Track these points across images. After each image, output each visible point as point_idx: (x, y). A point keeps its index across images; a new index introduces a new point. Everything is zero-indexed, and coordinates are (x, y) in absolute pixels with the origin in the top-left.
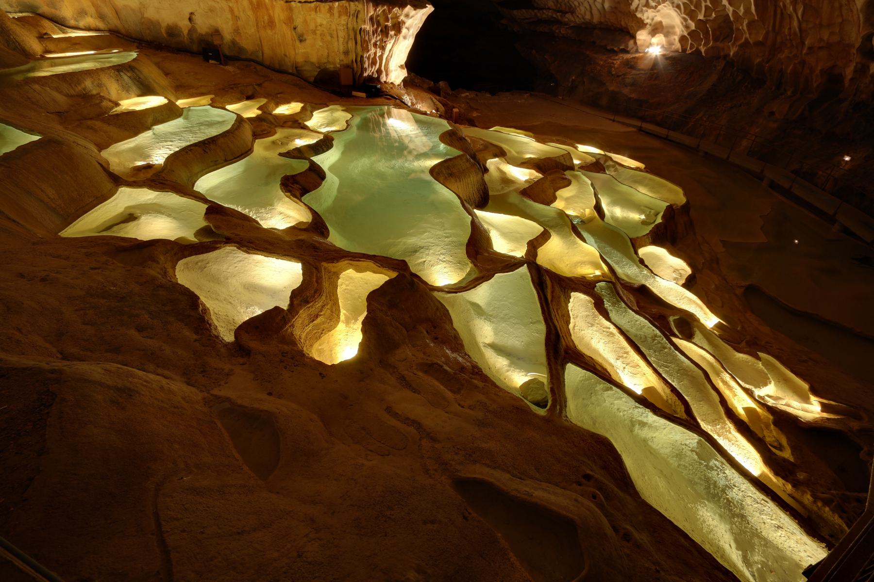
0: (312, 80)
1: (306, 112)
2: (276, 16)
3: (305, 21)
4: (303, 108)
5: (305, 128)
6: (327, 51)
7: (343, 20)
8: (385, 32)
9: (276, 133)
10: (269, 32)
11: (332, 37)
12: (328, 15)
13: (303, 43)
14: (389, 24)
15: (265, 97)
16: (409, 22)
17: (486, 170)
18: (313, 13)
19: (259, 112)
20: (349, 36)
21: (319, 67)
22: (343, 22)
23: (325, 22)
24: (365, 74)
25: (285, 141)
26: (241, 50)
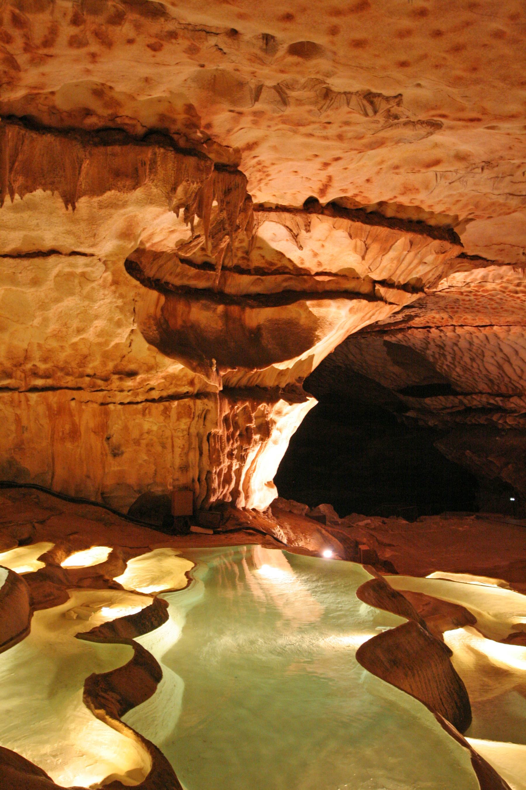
0: (125, 511)
1: (117, 562)
2: (83, 423)
3: (126, 428)
4: (111, 556)
5: (118, 587)
6: (153, 467)
7: (184, 423)
8: (246, 437)
9: (67, 598)
10: (69, 445)
11: (164, 447)
12: (162, 418)
13: (118, 459)
14: (253, 425)
15: (49, 541)
16: (280, 422)
17: (448, 652)
18: (140, 416)
19: (42, 565)
20: (190, 444)
21: (139, 491)
23: (155, 428)
24: (213, 499)
25: (83, 611)
26: (21, 472)
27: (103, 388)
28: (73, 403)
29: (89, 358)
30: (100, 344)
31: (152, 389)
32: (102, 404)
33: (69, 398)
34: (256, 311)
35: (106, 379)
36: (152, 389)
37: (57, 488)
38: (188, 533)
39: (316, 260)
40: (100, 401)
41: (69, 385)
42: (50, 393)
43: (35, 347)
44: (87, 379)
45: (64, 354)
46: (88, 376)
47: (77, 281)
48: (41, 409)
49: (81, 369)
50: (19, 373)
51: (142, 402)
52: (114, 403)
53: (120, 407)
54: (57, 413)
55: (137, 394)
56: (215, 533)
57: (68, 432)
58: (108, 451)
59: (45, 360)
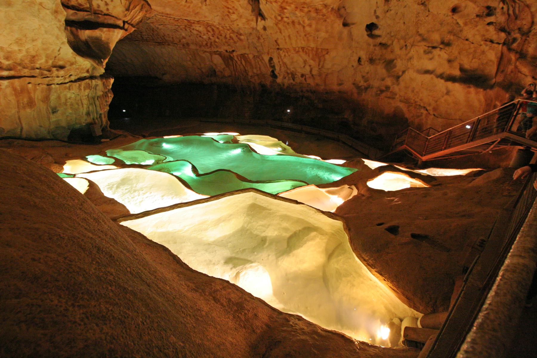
2: (36, 96)
3: (59, 97)
7: (87, 92)
10: (28, 110)
11: (78, 104)
13: (55, 114)
18: (67, 90)
21: (69, 129)
22: (87, 94)
23: (73, 96)
28: (30, 86)
29: (37, 58)
30: (45, 49)
31: (71, 75)
32: (48, 85)
34: (83, 31)
36: (71, 75)
37: (24, 135)
38: (101, 143)
39: (106, 7)
40: (47, 83)
41: (26, 75)
42: (16, 80)
44: (38, 70)
45: (21, 55)
46: (37, 69)
47: (37, 7)
48: (9, 91)
49: (32, 65)
51: (67, 83)
53: (58, 86)
55: (65, 79)
56: (111, 140)
57: (26, 102)
58: (51, 111)
59: (7, 58)
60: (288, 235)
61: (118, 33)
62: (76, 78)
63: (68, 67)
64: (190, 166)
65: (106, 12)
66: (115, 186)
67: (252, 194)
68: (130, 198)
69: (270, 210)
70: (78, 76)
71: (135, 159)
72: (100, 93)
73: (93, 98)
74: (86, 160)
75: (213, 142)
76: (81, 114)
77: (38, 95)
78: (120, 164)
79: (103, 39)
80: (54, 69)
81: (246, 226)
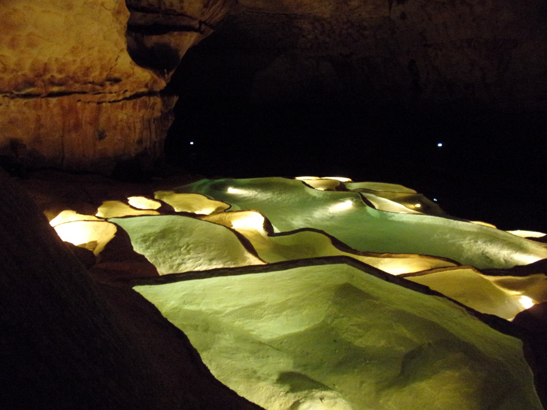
3: (109, 118)
10: (73, 135)
12: (132, 110)
18: (120, 110)
22: (141, 115)
27: (101, 91)
28: (79, 104)
29: (91, 69)
31: (126, 91)
33: (77, 100)
35: (102, 85)
36: (126, 91)
40: (97, 101)
43: (53, 62)
44: (90, 85)
46: (90, 83)
48: (56, 110)
49: (85, 78)
50: (40, 83)
52: (105, 102)
53: (109, 104)
54: (67, 112)
55: (118, 95)
58: (97, 136)
59: (60, 71)
60: (403, 349)
61: (191, 37)
62: (132, 94)
63: (124, 81)
64: (263, 219)
65: (179, 11)
66: (152, 238)
67: (345, 266)
68: (167, 257)
69: (377, 299)
70: (134, 92)
71: (189, 206)
72: (157, 114)
73: (149, 121)
74: (126, 202)
75: (304, 187)
76: (132, 142)
77: (86, 115)
78: (166, 210)
79: (172, 45)
80: (108, 83)
81: (329, 322)
